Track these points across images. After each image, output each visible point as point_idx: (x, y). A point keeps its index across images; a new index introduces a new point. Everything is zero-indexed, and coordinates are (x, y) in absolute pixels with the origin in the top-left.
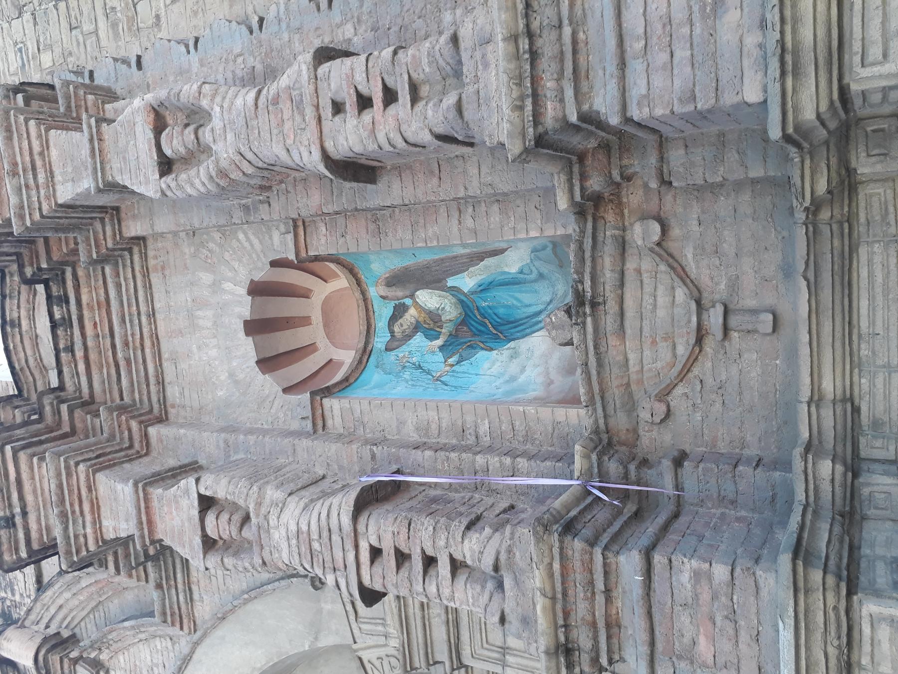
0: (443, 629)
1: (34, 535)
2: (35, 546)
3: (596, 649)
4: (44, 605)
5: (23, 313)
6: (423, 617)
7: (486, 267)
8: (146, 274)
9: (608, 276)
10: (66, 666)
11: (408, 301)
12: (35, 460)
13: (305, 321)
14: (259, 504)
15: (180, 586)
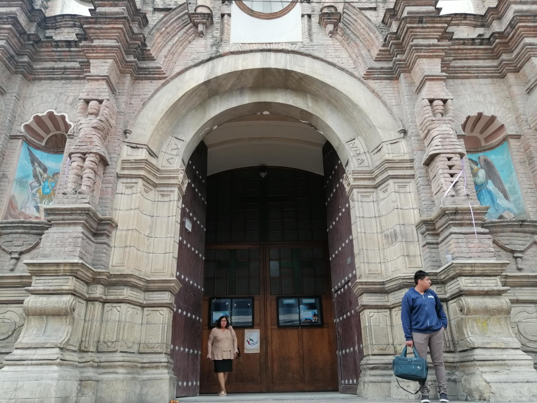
0: (403, 174)
1: (415, 30)
2: (411, 30)
3: (456, 220)
4: (357, 14)
5: (468, 22)
6: (403, 167)
7: (498, 193)
8: (491, 77)
9: (527, 229)
10: (334, 20)
11: (479, 166)
12: (440, 34)
13: (472, 131)
14: (451, 120)
15: (380, 76)
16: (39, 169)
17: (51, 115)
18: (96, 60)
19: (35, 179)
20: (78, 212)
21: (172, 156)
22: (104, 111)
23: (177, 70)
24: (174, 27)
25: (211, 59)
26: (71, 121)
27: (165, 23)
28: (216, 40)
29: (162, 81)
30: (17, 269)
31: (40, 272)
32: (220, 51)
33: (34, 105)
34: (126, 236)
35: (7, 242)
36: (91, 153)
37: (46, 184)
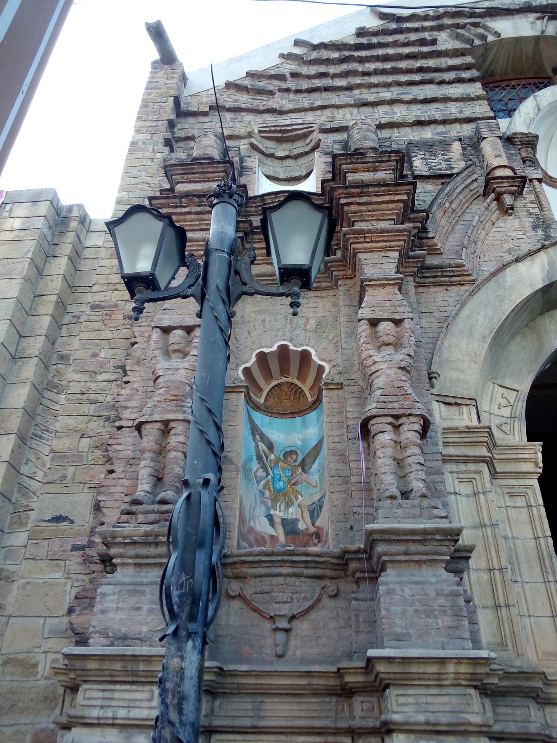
16: (262, 446)
17: (283, 350)
18: (369, 255)
19: (259, 463)
20: (438, 537)
21: (504, 420)
22: (412, 339)
23: (488, 268)
24: (461, 201)
25: (543, 247)
26: (323, 360)
27: (449, 194)
28: (538, 219)
29: (466, 287)
30: (290, 653)
31: (402, 676)
32: (553, 235)
33: (253, 334)
34: (492, 582)
35: (261, 593)
36: (410, 415)
37: (277, 472)
